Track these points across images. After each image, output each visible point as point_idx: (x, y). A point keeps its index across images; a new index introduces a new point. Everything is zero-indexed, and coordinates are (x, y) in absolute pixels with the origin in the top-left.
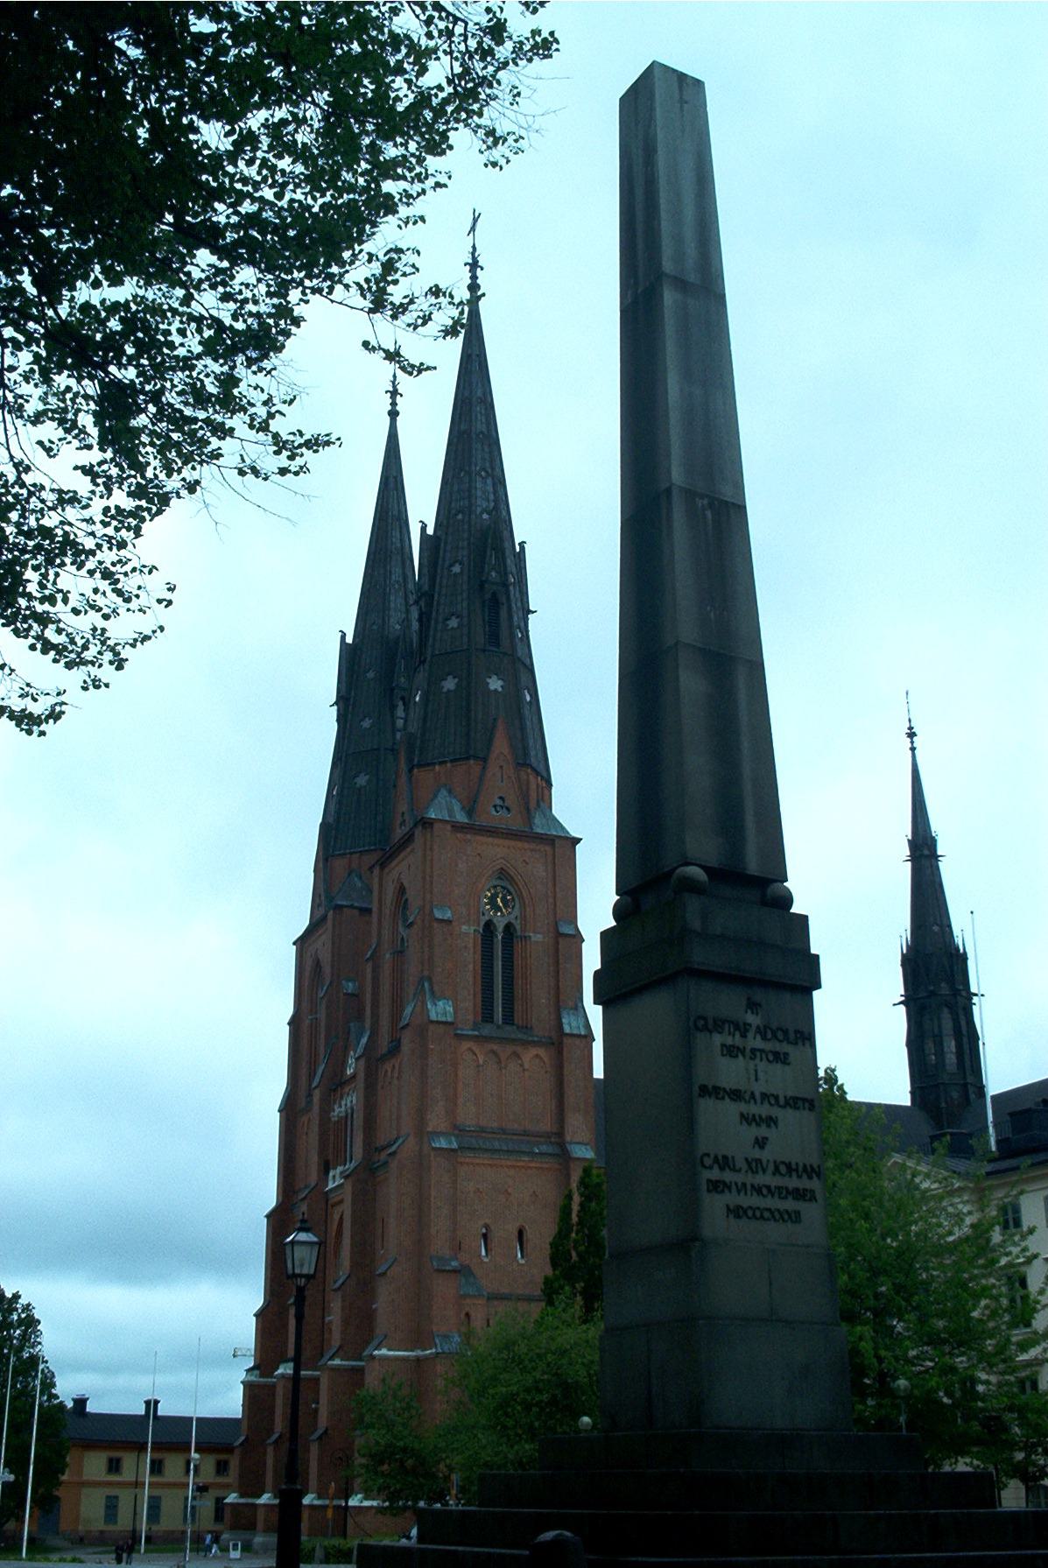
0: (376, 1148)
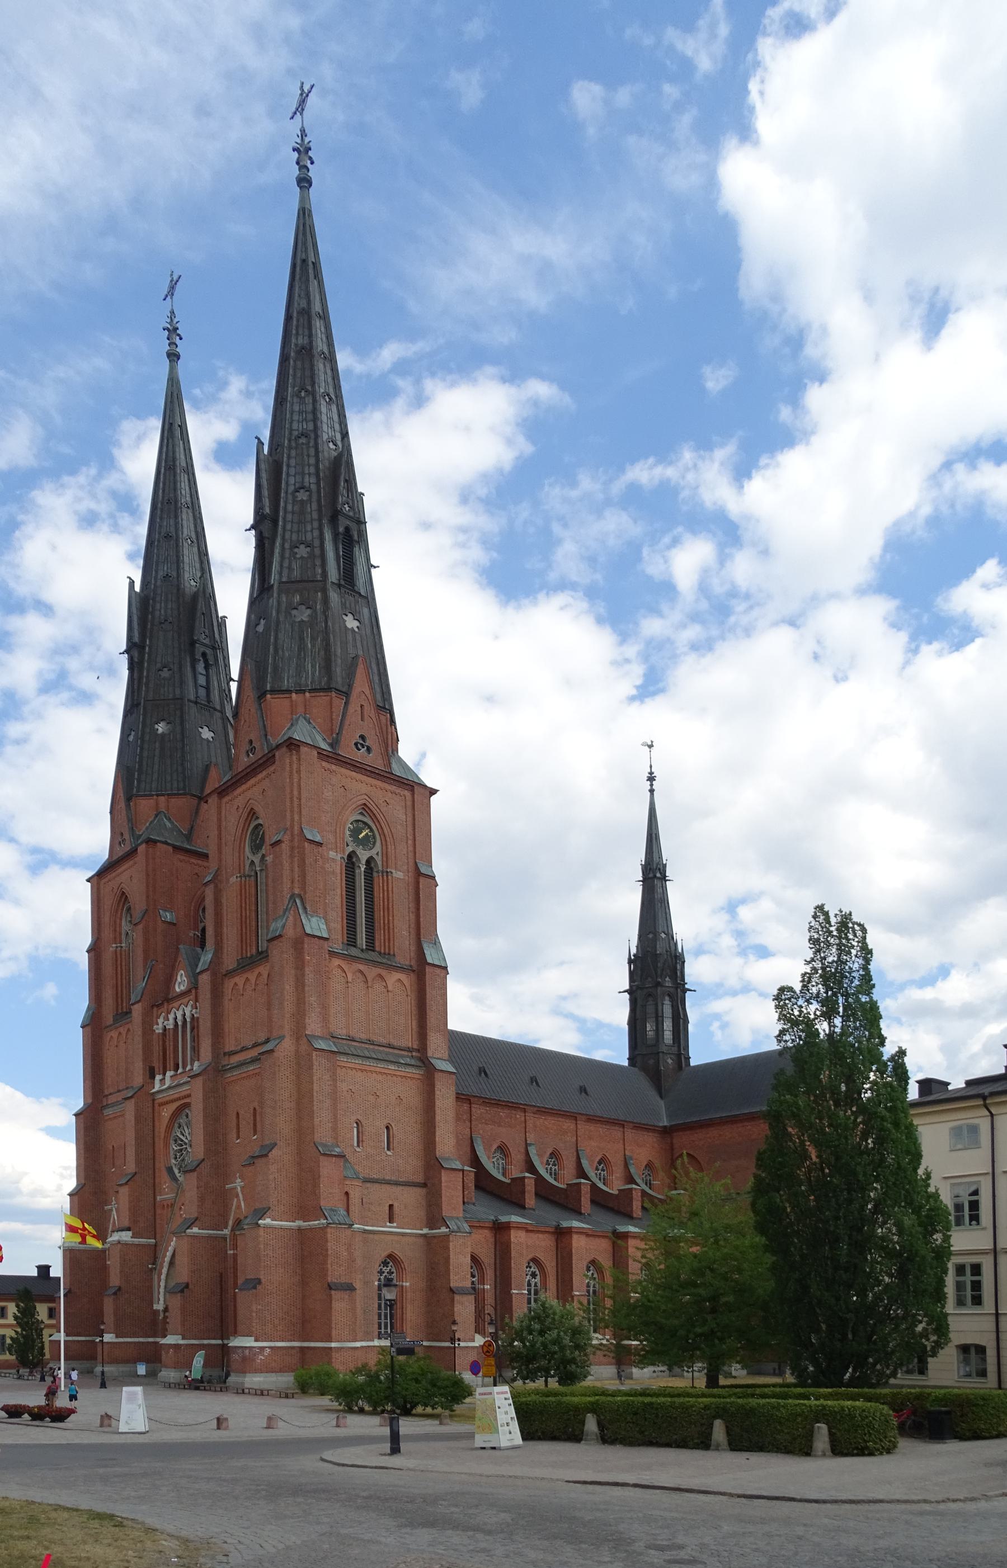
0: (225, 1054)
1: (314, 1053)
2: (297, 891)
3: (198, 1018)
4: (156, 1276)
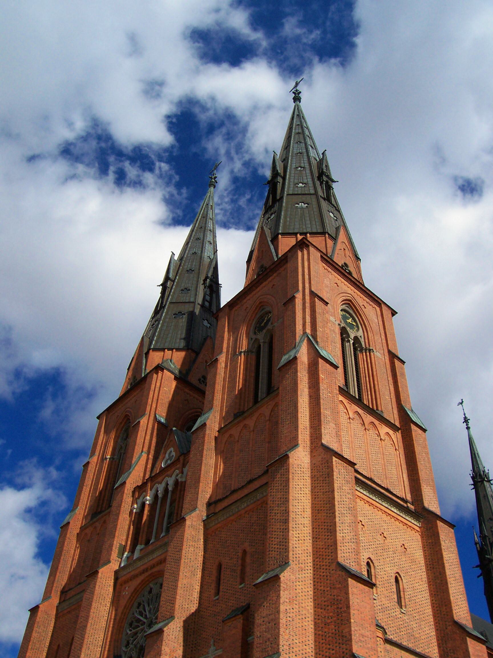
3: (182, 482)
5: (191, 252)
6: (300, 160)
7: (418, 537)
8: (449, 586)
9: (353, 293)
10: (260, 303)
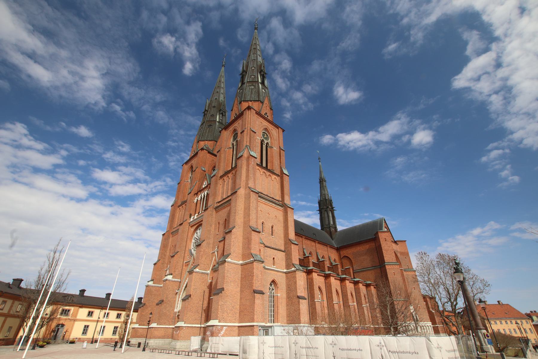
1: (251, 192)
2: (248, 144)
3: (209, 194)
4: (178, 296)
5: (215, 98)
6: (254, 63)
7: (282, 213)
8: (289, 228)
9: (267, 125)
10: (235, 129)
